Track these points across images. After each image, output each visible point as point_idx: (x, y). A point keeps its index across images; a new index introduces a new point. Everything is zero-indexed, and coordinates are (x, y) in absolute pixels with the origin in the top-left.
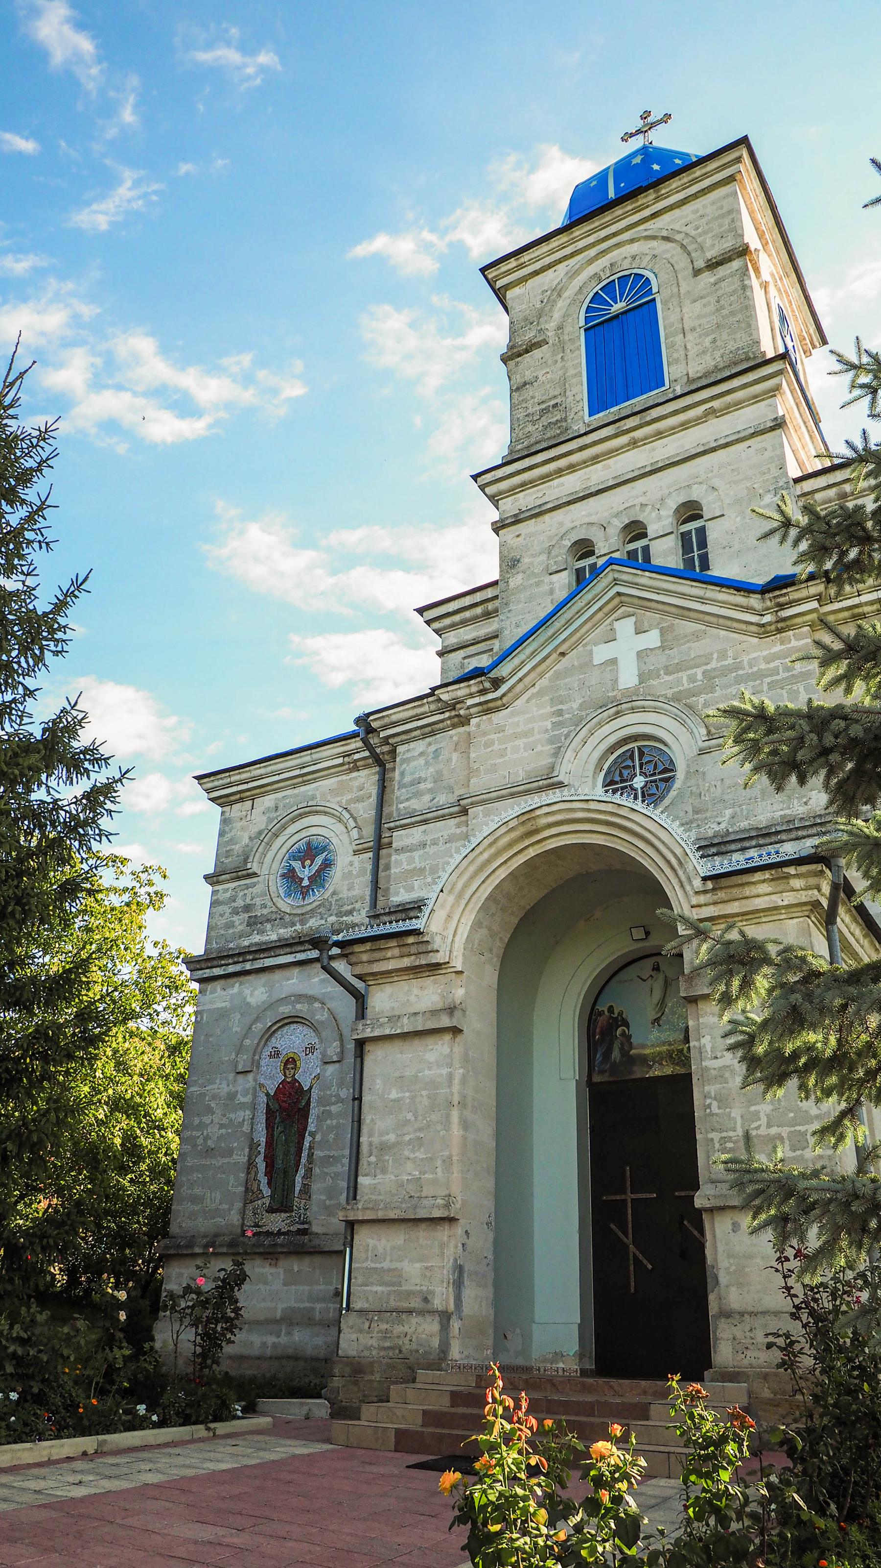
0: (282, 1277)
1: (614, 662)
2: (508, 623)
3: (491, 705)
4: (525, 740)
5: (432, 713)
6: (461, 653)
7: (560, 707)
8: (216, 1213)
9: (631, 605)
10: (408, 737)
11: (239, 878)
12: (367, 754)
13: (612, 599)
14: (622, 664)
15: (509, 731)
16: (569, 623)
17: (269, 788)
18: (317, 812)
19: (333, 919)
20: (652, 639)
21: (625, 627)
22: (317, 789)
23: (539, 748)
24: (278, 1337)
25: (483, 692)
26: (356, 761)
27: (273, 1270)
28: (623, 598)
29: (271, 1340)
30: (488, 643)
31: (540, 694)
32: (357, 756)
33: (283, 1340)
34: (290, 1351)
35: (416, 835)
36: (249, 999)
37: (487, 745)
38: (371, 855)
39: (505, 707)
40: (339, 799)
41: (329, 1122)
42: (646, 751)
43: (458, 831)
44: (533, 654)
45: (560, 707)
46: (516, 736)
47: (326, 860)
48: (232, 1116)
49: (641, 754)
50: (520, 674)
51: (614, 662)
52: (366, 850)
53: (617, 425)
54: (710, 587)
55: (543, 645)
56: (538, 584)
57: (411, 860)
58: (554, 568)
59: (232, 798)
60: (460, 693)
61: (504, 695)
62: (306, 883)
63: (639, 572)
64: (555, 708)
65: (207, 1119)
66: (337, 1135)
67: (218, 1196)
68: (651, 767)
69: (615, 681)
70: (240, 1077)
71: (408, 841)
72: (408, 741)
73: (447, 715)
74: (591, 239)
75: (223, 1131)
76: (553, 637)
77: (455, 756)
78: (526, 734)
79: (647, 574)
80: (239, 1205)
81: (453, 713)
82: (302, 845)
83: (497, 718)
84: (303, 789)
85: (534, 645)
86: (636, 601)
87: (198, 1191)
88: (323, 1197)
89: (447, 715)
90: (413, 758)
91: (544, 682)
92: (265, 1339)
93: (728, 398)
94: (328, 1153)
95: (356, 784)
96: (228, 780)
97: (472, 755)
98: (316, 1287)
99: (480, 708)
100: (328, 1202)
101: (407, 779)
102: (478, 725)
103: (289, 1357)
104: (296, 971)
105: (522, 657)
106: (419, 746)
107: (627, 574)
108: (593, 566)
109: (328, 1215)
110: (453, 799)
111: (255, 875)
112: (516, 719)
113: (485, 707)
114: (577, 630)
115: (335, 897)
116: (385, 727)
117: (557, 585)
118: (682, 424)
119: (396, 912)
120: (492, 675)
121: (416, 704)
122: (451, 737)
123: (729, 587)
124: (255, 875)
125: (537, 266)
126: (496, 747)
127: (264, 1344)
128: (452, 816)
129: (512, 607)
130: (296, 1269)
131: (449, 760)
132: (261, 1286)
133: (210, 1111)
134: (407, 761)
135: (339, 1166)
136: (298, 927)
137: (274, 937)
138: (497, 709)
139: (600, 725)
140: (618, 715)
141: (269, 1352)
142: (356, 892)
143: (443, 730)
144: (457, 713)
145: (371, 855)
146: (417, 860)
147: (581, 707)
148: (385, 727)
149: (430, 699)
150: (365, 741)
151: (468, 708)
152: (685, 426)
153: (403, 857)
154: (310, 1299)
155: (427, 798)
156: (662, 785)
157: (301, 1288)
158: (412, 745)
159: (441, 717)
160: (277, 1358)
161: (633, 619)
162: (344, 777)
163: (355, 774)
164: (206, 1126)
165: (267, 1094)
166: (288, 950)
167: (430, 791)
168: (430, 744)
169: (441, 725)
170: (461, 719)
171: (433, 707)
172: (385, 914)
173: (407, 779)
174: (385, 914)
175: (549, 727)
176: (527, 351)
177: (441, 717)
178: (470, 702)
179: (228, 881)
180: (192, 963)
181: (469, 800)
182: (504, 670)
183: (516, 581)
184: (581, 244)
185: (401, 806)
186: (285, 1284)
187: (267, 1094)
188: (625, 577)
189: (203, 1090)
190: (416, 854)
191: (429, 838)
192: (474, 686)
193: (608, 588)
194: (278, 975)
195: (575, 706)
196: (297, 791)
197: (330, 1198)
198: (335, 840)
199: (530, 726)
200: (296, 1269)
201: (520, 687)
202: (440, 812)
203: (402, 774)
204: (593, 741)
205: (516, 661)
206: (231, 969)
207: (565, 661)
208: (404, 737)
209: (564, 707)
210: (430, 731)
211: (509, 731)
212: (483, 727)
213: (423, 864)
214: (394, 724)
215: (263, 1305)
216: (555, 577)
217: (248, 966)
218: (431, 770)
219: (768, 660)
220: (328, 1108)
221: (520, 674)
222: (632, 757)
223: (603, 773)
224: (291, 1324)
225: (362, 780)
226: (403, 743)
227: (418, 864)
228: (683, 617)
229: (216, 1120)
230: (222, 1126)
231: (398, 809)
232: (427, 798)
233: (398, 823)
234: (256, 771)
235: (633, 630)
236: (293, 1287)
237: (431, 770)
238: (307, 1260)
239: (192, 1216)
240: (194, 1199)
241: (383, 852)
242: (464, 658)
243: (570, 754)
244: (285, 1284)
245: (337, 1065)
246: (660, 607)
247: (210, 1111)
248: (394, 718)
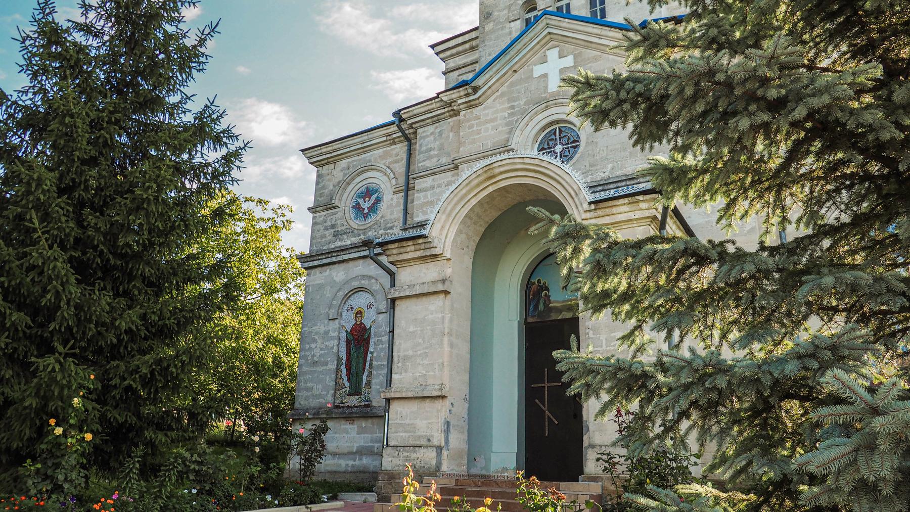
0: (356, 429)
1: (545, 76)
2: (484, 53)
3: (472, 103)
4: (492, 124)
6: (457, 73)
7: (513, 104)
8: (320, 396)
9: (557, 40)
10: (424, 123)
11: (328, 209)
12: (400, 134)
13: (545, 36)
14: (550, 77)
15: (483, 119)
16: (519, 52)
17: (344, 156)
18: (372, 170)
19: (382, 232)
20: (569, 61)
21: (553, 54)
22: (372, 156)
23: (500, 129)
24: (355, 461)
25: (467, 95)
26: (394, 139)
27: (351, 426)
28: (552, 36)
29: (351, 463)
30: (473, 66)
31: (502, 95)
32: (394, 136)
33: (357, 463)
34: (362, 469)
35: (429, 181)
36: (335, 278)
37: (470, 128)
38: (403, 194)
39: (480, 104)
40: (384, 162)
41: (381, 346)
42: (563, 129)
44: (498, 71)
45: (513, 104)
46: (487, 122)
47: (377, 197)
48: (327, 343)
49: (561, 132)
50: (490, 84)
51: (545, 76)
52: (400, 191)
54: (604, 28)
55: (504, 66)
56: (502, 29)
57: (425, 197)
58: (512, 18)
59: (323, 162)
60: (454, 96)
61: (480, 97)
62: (366, 211)
63: (562, 19)
64: (510, 105)
65: (313, 346)
67: (320, 387)
68: (566, 139)
69: (546, 87)
70: (331, 322)
71: (424, 185)
72: (424, 126)
73: (446, 109)
75: (323, 352)
76: (510, 60)
77: (451, 134)
78: (493, 120)
79: (567, 20)
80: (332, 392)
81: (450, 108)
82: (364, 189)
83: (476, 111)
84: (364, 156)
85: (498, 66)
86: (560, 38)
87: (309, 385)
89: (446, 109)
90: (427, 136)
91: (504, 89)
92: (347, 462)
94: (380, 363)
95: (394, 152)
96: (320, 152)
97: (461, 134)
98: (375, 435)
99: (466, 105)
101: (424, 148)
102: (465, 116)
103: (360, 472)
104: (361, 262)
105: (491, 73)
106: (430, 129)
107: (554, 20)
108: (535, 17)
110: (450, 160)
111: (337, 207)
112: (487, 112)
113: (469, 104)
114: (524, 56)
115: (383, 219)
116: (410, 118)
117: (514, 29)
120: (473, 84)
122: (449, 123)
123: (616, 28)
124: (337, 207)
126: (475, 128)
127: (347, 465)
128: (449, 170)
129: (486, 43)
130: (364, 425)
132: (345, 435)
133: (315, 341)
134: (424, 138)
136: (362, 237)
137: (348, 243)
138: (476, 106)
139: (536, 114)
140: (547, 108)
141: (350, 469)
142: (395, 216)
143: (444, 119)
145: (403, 194)
146: (429, 196)
147: (526, 104)
148: (410, 118)
149: (437, 100)
150: (398, 126)
151: (459, 105)
153: (421, 195)
154: (372, 441)
155: (435, 159)
156: (572, 150)
157: (366, 435)
158: (426, 128)
159: (443, 111)
160: (354, 472)
161: (558, 49)
162: (388, 149)
163: (394, 147)
164: (313, 349)
166: (356, 250)
167: (437, 155)
168: (437, 128)
171: (438, 105)
173: (424, 148)
175: (507, 116)
177: (443, 111)
178: (460, 101)
179: (322, 211)
180: (302, 258)
181: (459, 161)
182: (480, 82)
183: (489, 26)
185: (420, 165)
186: (358, 434)
187: (347, 331)
188: (553, 22)
189: (311, 330)
190: (429, 193)
191: (436, 183)
192: (462, 91)
193: (543, 29)
194: (351, 264)
195: (522, 103)
196: (360, 157)
198: (382, 186)
199: (495, 115)
200: (364, 425)
201: (490, 91)
203: (421, 146)
204: (532, 124)
205: (487, 76)
206: (325, 261)
207: (516, 76)
208: (421, 123)
209: (515, 104)
210: (437, 120)
211: (483, 119)
212: (467, 117)
213: (432, 199)
214: (415, 116)
215: (347, 444)
216: (513, 24)
217: (334, 259)
218: (438, 143)
221: (490, 84)
222: (555, 134)
223: (538, 143)
224: (362, 455)
225: (397, 150)
226: (421, 127)
227: (430, 199)
228: (587, 48)
229: (318, 346)
230: (322, 349)
231: (418, 167)
232: (435, 159)
233: (418, 175)
234: (336, 146)
235: (557, 55)
236: (362, 435)
237: (438, 143)
238: (370, 421)
239: (307, 398)
240: (307, 389)
241: (410, 192)
242: (459, 75)
243: (518, 132)
244: (358, 434)
245: (385, 314)
246: (574, 41)
247: (315, 341)
248: (415, 112)
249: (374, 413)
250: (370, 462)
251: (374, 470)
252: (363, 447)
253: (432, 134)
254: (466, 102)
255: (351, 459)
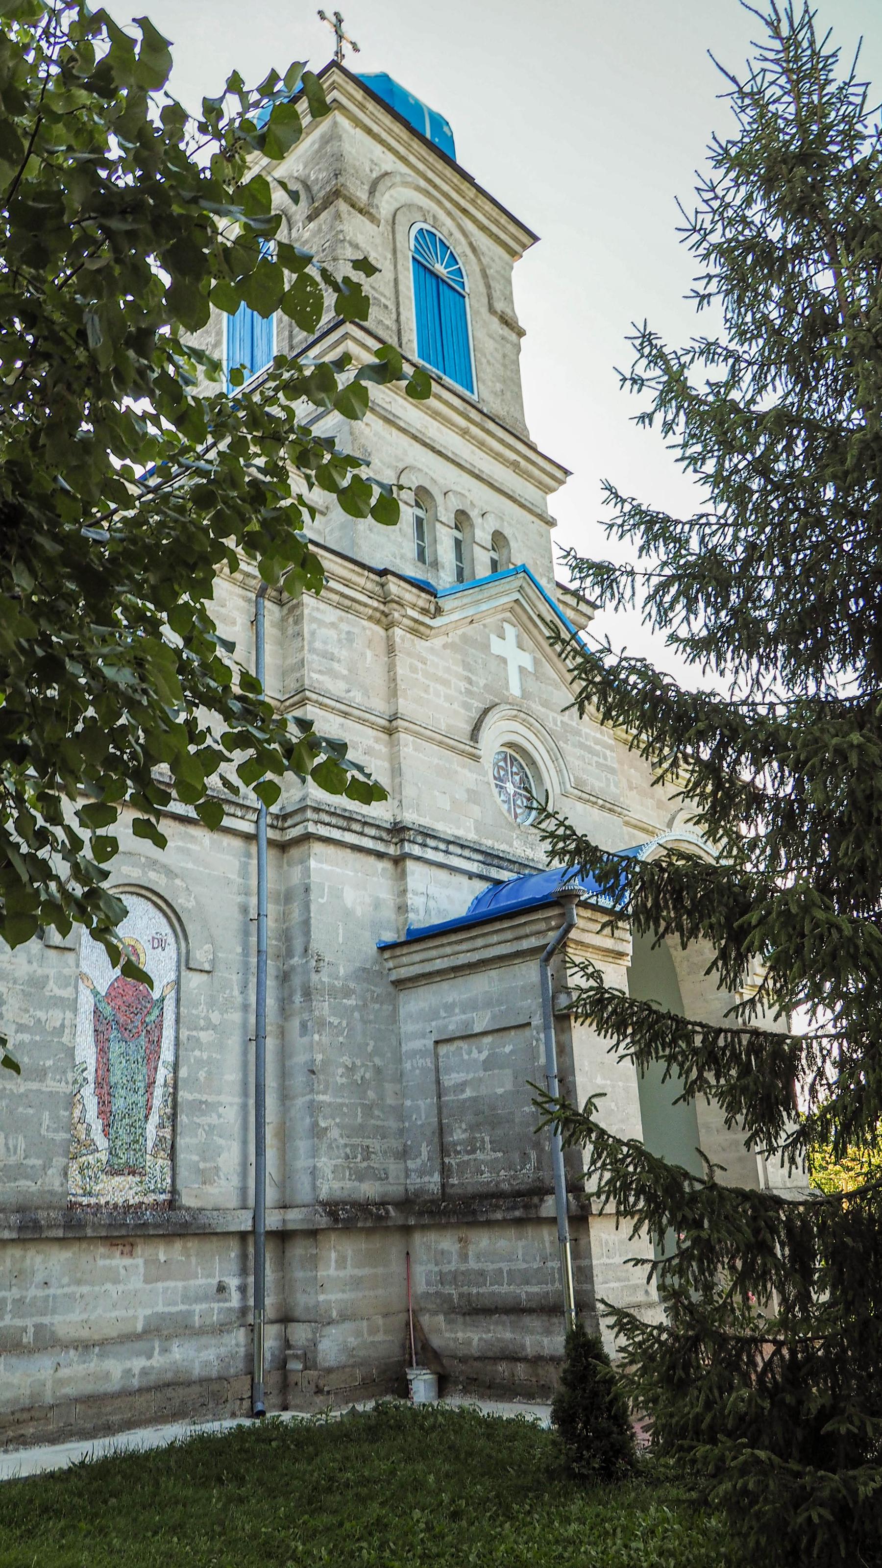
3: (422, 629)
5: (363, 590)
25: (424, 611)
41: (197, 1053)
43: (377, 747)
53: (469, 408)
64: (465, 673)
66: (209, 1073)
70: (52, 953)
73: (375, 604)
74: (421, 166)
81: (382, 607)
88: (195, 1158)
93: (531, 468)
94: (197, 1096)
98: (192, 1282)
100: (202, 1165)
109: (204, 1183)
113: (416, 626)
118: (498, 454)
119: (339, 815)
121: (356, 568)
125: (376, 128)
128: (372, 726)
131: (363, 655)
135: (214, 1115)
138: (421, 636)
143: (358, 614)
144: (386, 610)
149: (372, 576)
152: (497, 457)
154: (186, 1299)
159: (369, 601)
165: (96, 994)
169: (361, 609)
170: (383, 619)
171: (370, 586)
172: (328, 812)
174: (328, 812)
176: (361, 211)
177: (369, 601)
178: (410, 612)
181: (406, 724)
184: (412, 159)
187: (96, 994)
197: (204, 1160)
200: (162, 1258)
202: (367, 716)
209: (474, 678)
219: (597, 742)
220: (194, 1033)
236: (160, 1285)
238: (178, 1245)
249: (204, 1226)
250: (192, 1353)
251: (203, 1373)
252: (162, 1316)
253: (333, 625)
254: (416, 621)
255: (138, 1354)
